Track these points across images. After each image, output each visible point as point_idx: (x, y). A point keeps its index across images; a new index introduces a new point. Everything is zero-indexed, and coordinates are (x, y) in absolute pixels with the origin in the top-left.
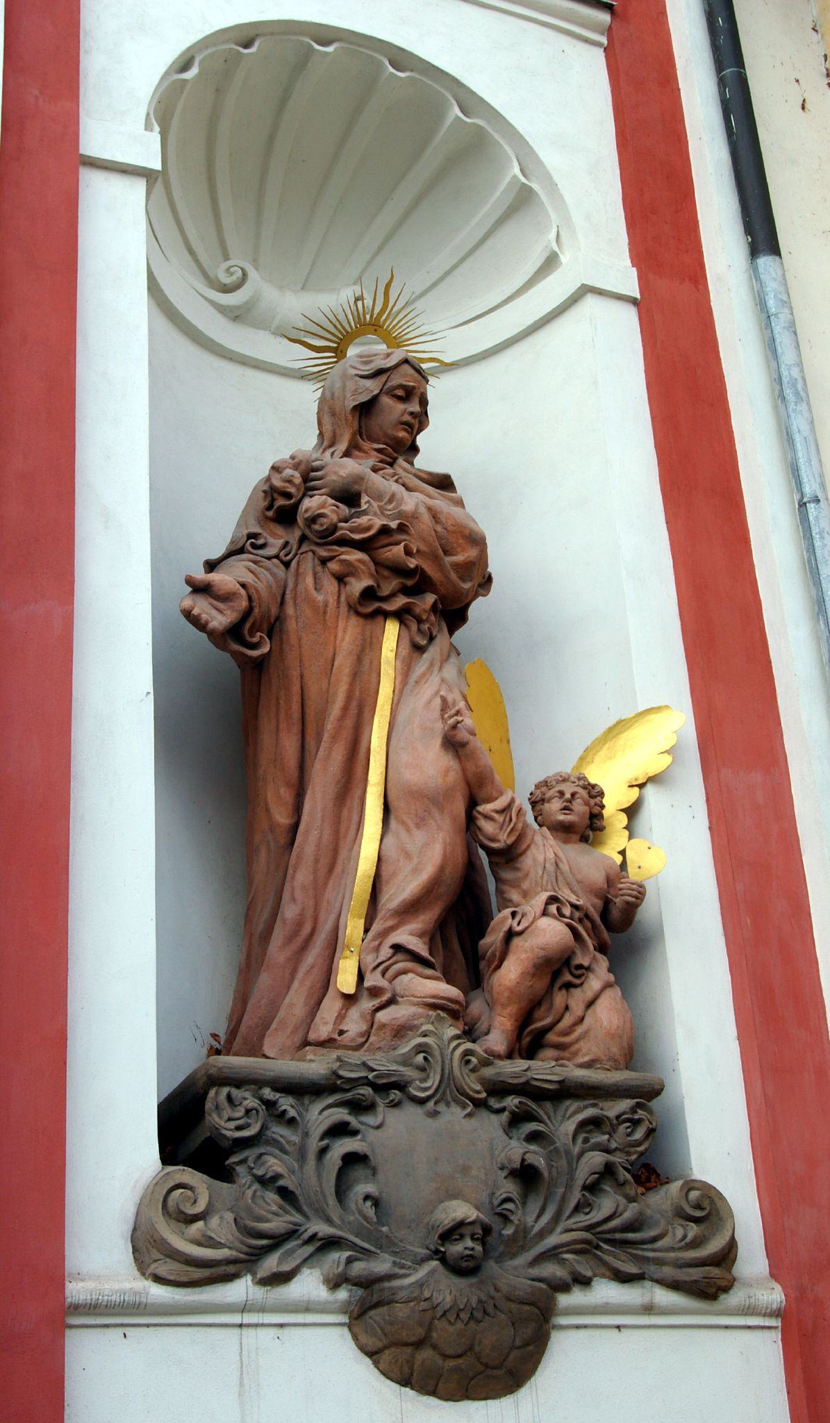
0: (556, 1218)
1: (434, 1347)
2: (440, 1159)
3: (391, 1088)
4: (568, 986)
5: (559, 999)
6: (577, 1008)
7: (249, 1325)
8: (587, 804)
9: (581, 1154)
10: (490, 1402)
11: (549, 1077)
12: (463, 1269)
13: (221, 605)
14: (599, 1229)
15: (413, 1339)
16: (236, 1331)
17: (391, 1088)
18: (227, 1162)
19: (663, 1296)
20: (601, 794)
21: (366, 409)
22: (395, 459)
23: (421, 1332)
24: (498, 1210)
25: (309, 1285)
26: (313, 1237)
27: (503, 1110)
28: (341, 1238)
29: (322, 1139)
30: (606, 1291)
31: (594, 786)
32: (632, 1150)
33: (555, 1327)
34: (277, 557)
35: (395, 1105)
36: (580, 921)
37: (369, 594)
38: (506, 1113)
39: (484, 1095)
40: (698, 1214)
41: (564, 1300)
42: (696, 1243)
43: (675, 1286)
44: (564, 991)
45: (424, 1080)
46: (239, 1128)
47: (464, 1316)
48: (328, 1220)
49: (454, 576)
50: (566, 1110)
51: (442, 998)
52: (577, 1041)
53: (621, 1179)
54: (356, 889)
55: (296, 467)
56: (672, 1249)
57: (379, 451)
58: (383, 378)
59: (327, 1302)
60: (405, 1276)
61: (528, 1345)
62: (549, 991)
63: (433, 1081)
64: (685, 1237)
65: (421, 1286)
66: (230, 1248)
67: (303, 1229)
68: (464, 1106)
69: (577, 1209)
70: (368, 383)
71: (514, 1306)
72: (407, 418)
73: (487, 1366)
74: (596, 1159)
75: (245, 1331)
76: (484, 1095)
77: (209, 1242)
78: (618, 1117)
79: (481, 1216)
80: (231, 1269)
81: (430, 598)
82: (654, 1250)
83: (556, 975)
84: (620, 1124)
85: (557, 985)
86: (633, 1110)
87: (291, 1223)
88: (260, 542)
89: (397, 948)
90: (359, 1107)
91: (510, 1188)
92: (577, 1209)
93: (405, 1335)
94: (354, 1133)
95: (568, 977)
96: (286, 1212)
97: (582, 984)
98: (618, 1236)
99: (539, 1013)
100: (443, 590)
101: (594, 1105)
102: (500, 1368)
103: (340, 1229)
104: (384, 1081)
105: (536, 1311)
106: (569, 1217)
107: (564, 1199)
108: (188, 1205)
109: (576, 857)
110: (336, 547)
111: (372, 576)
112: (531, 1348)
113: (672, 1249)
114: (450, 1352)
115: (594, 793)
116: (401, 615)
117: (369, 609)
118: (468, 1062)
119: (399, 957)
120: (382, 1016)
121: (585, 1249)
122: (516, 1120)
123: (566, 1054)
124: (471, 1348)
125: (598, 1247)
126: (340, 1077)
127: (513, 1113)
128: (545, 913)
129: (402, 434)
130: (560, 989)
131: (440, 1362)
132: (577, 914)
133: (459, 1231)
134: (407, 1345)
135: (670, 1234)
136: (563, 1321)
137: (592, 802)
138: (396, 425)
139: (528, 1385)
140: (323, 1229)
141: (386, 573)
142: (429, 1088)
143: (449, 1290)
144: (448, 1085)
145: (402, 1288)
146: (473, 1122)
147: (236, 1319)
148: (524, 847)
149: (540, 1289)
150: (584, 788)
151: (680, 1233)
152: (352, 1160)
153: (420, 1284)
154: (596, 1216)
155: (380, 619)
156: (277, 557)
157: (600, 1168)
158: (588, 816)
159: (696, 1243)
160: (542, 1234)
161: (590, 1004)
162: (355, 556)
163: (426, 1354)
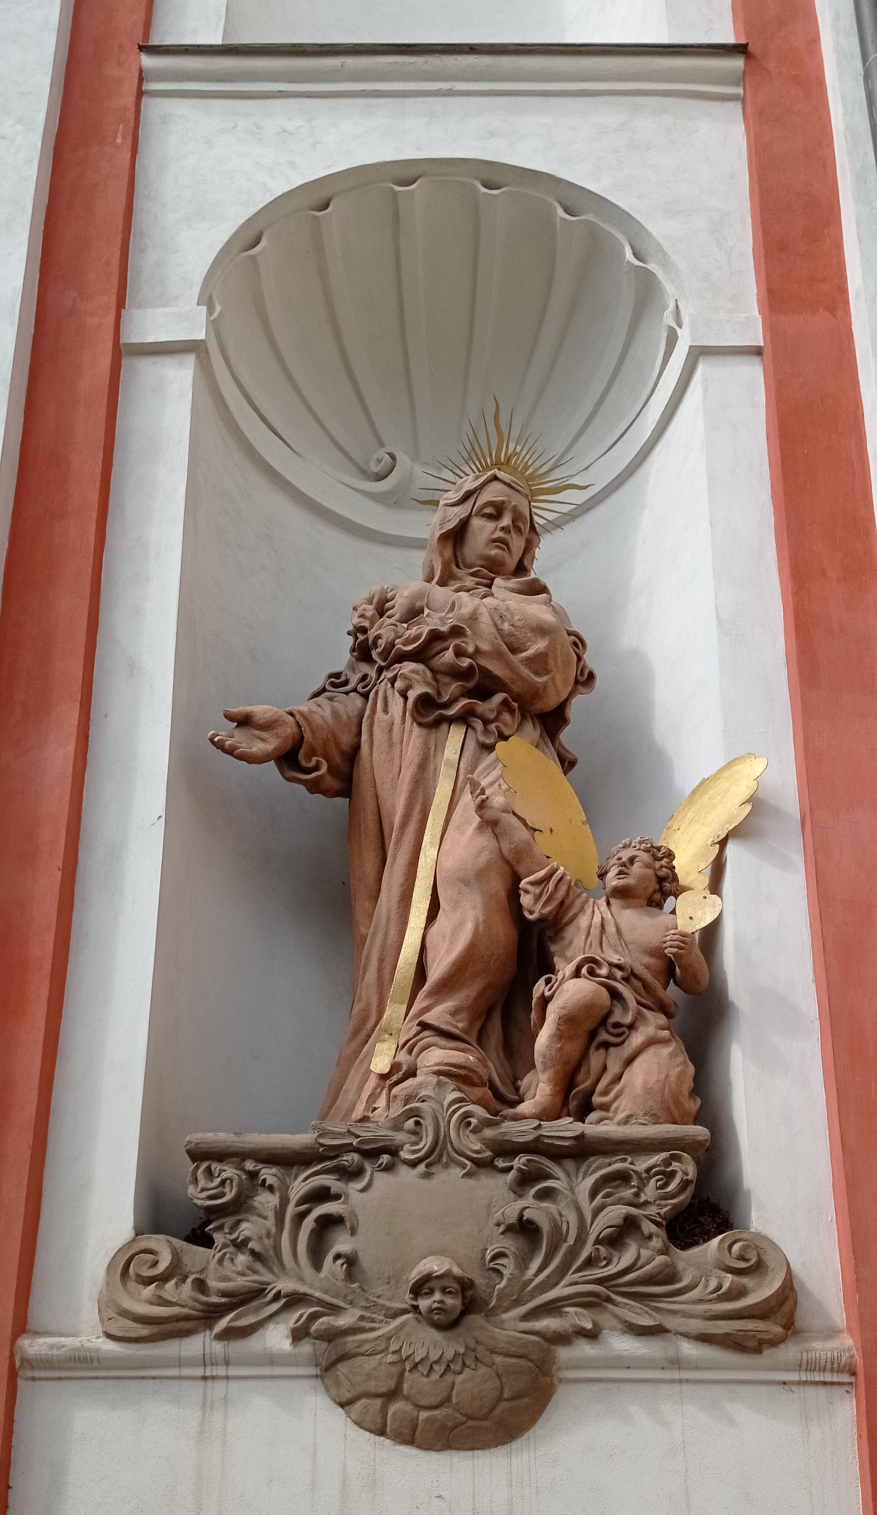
0: (563, 1270)
1: (407, 1398)
2: (424, 1220)
3: (380, 1153)
4: (606, 1045)
5: (596, 1059)
6: (613, 1068)
7: (213, 1378)
8: (647, 866)
9: (602, 1208)
10: (480, 1453)
11: (562, 1134)
12: (448, 1324)
13: (264, 735)
14: (612, 1283)
15: (384, 1390)
16: (201, 1383)
17: (380, 1153)
18: (207, 1229)
19: (689, 1349)
20: (670, 855)
21: (457, 536)
23: (392, 1384)
24: (492, 1265)
25: (277, 1337)
26: (277, 1297)
28: (306, 1294)
29: (298, 1204)
30: (623, 1345)
31: (659, 849)
32: (663, 1202)
33: (561, 1381)
35: (388, 1168)
36: (626, 980)
37: (425, 703)
38: (513, 1171)
39: (489, 1153)
40: (742, 1265)
41: (563, 1353)
42: (738, 1293)
43: (704, 1338)
44: (602, 1051)
45: (417, 1143)
46: (211, 1198)
47: (439, 1369)
48: (301, 1279)
49: (525, 672)
50: (589, 1167)
51: (446, 1064)
52: (616, 1097)
53: (646, 1232)
55: (370, 602)
56: (701, 1301)
58: (471, 502)
59: (289, 1355)
60: (373, 1329)
62: (584, 1056)
63: (427, 1142)
64: (719, 1287)
65: (389, 1339)
66: (190, 1308)
67: (270, 1287)
68: (464, 1166)
69: (590, 1262)
70: (456, 510)
71: (498, 1359)
72: (499, 534)
73: (470, 1417)
74: (615, 1213)
75: (210, 1383)
76: (489, 1153)
77: (163, 1302)
78: (648, 1170)
79: (456, 1270)
80: (186, 1325)
81: (498, 698)
83: (593, 1034)
84: (651, 1178)
85: (594, 1045)
86: (667, 1162)
87: (255, 1282)
90: (351, 1174)
91: (509, 1244)
92: (590, 1262)
93: (372, 1386)
94: (337, 1197)
95: (604, 1036)
96: (255, 1272)
97: (623, 1042)
98: (634, 1289)
99: (580, 1077)
100: (515, 688)
101: (625, 1160)
102: (485, 1418)
103: (311, 1287)
105: (531, 1364)
106: (578, 1270)
107: (574, 1252)
108: (145, 1268)
109: (634, 922)
110: (397, 665)
111: (427, 684)
112: (525, 1400)
113: (701, 1301)
114: (425, 1402)
115: (660, 855)
116: (464, 718)
117: (431, 718)
118: (469, 1124)
119: (426, 1033)
120: (395, 1091)
121: (591, 1302)
122: (525, 1180)
123: (610, 1114)
124: (448, 1399)
125: (609, 1300)
126: (322, 1145)
127: (520, 1170)
128: (577, 974)
129: (494, 552)
130: (598, 1048)
131: (415, 1413)
132: (619, 974)
134: (377, 1396)
136: (571, 1374)
137: (658, 865)
138: (487, 544)
140: (286, 1285)
141: (446, 680)
143: (427, 1342)
144: (444, 1147)
145: (365, 1341)
146: (471, 1182)
147: (199, 1372)
148: (571, 914)
149: (533, 1342)
150: (647, 851)
151: (713, 1284)
152: (328, 1223)
153: (388, 1338)
154: (612, 1270)
155: (444, 727)
157: (620, 1221)
158: (654, 878)
159: (738, 1293)
160: (543, 1287)
162: (408, 667)
163: (397, 1407)
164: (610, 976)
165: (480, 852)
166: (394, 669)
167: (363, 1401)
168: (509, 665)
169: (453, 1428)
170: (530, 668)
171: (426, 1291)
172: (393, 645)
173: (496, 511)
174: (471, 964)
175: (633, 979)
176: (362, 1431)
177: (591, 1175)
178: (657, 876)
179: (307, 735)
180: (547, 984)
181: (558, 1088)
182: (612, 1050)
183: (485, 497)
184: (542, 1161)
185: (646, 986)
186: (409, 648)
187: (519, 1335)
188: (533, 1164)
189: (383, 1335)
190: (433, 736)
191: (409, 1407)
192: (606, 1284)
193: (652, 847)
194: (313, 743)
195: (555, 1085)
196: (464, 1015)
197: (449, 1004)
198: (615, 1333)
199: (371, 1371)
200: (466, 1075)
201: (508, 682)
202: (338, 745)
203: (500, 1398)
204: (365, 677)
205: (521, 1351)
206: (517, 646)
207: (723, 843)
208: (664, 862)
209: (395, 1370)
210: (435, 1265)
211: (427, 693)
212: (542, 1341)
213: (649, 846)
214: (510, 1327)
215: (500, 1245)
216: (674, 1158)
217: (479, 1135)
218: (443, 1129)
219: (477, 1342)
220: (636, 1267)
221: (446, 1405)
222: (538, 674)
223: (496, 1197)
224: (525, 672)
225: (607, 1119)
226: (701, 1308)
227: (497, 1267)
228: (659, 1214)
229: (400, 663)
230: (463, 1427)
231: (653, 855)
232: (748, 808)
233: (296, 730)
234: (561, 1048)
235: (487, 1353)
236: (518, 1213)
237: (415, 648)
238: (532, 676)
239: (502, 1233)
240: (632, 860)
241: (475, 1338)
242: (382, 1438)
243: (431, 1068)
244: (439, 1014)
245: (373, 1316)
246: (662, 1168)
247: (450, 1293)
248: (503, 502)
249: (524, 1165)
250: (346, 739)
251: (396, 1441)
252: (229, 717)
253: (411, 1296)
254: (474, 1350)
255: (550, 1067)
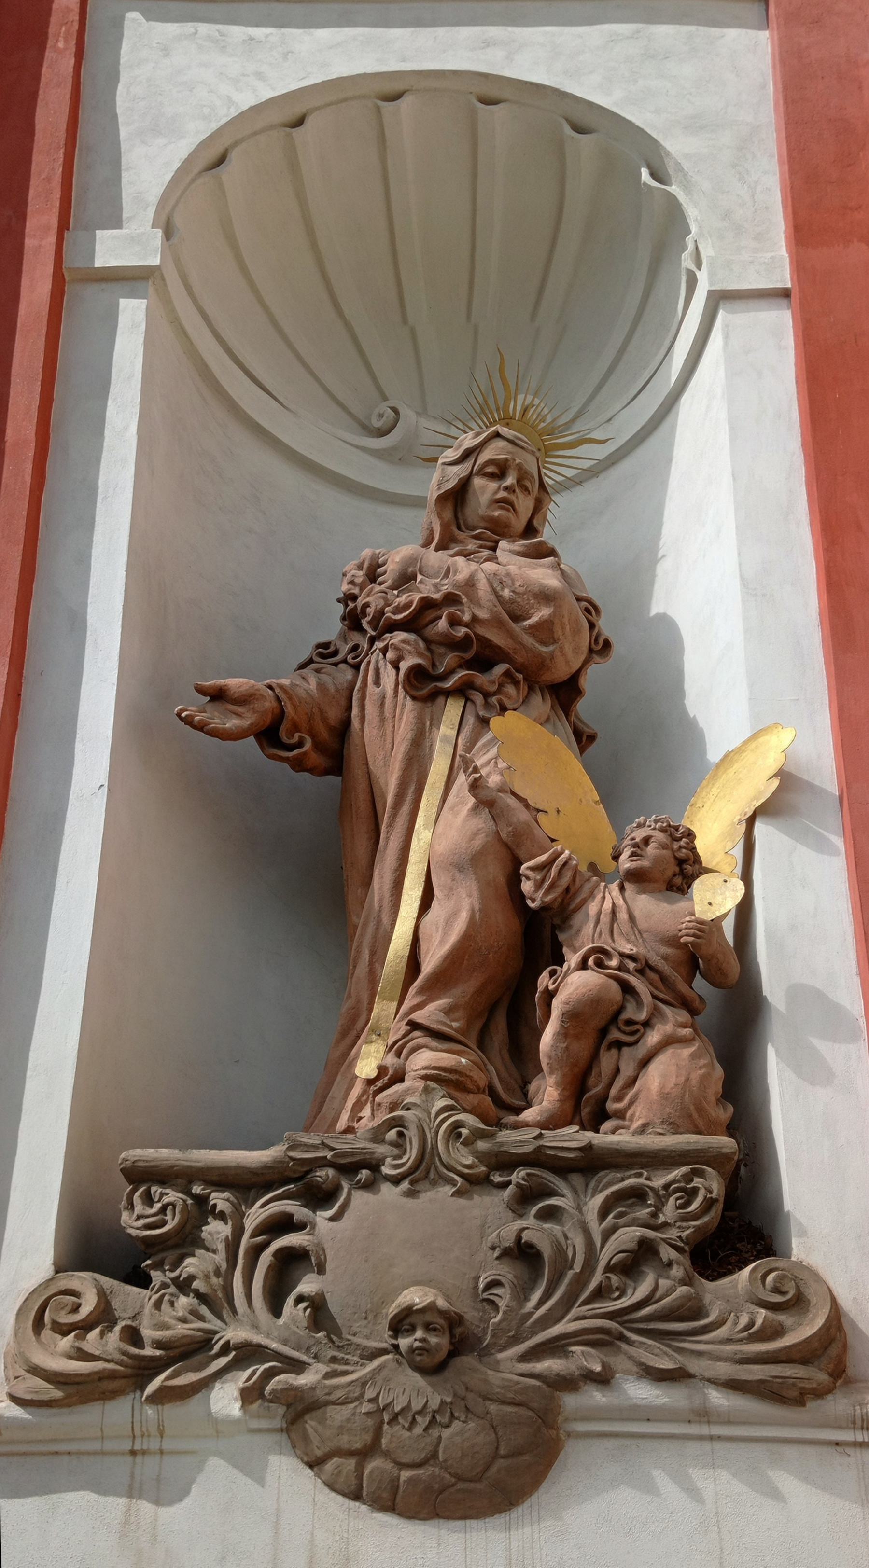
0: (568, 1303)
1: (387, 1454)
4: (619, 1045)
5: (607, 1060)
6: (627, 1069)
8: (664, 847)
9: (613, 1229)
11: (566, 1144)
12: (433, 1368)
13: (240, 709)
14: (626, 1318)
15: (358, 1446)
17: (361, 1169)
20: (690, 835)
21: (457, 497)
22: (497, 542)
23: (368, 1438)
24: (485, 1295)
27: (505, 1185)
31: (677, 828)
32: (684, 1224)
33: (569, 1435)
34: (345, 661)
35: (369, 1186)
36: (640, 972)
41: (570, 1401)
42: (773, 1332)
43: (734, 1385)
44: (614, 1051)
45: (400, 1157)
49: (528, 640)
51: (435, 1068)
52: (631, 1103)
54: (386, 970)
55: (360, 567)
56: (729, 1341)
57: (476, 537)
60: (346, 1373)
61: (520, 1454)
62: (594, 1057)
63: (411, 1155)
64: (751, 1324)
65: (364, 1384)
68: (453, 1183)
69: (600, 1294)
70: (455, 469)
71: (493, 1408)
73: (460, 1478)
74: (628, 1236)
76: (483, 1169)
78: (666, 1187)
79: (441, 1303)
81: (500, 669)
82: (707, 1343)
83: (603, 1032)
84: (670, 1196)
86: (688, 1178)
88: (332, 648)
89: (414, 1026)
91: (506, 1272)
92: (600, 1294)
93: (344, 1441)
95: (615, 1034)
97: (637, 1042)
99: (591, 1080)
100: (519, 659)
101: (640, 1175)
102: (478, 1479)
104: (348, 1160)
105: (531, 1413)
106: (586, 1302)
107: (581, 1280)
109: (648, 907)
110: (387, 635)
111: (420, 655)
112: (526, 1457)
113: (729, 1341)
114: (406, 1459)
115: (678, 834)
116: (463, 691)
117: (425, 692)
118: (459, 1135)
119: (417, 1033)
120: (378, 1098)
121: (601, 1340)
122: (526, 1197)
123: (626, 1123)
124: (434, 1455)
125: (622, 1338)
127: (518, 1185)
128: (583, 965)
130: (609, 1047)
131: (395, 1472)
132: (631, 965)
133: (408, 1321)
134: (351, 1453)
135: (729, 1323)
137: (676, 846)
139: (526, 1504)
141: (442, 650)
142: (403, 1165)
143: (410, 1389)
145: (336, 1387)
146: (462, 1202)
148: (578, 900)
149: (534, 1386)
150: (663, 830)
151: (744, 1320)
153: (363, 1383)
154: (625, 1302)
155: (441, 700)
156: (345, 661)
157: (633, 1245)
158: (672, 860)
159: (773, 1332)
161: (645, 1063)
162: (399, 637)
163: (374, 1464)
164: (621, 968)
165: (476, 834)
166: (384, 639)
167: (336, 1460)
168: (511, 634)
169: (441, 1492)
170: (534, 636)
171: (406, 1327)
172: (381, 613)
173: (499, 470)
174: (467, 957)
175: (648, 971)
176: (333, 1495)
177: (601, 1191)
178: (675, 858)
179: (289, 709)
180: (551, 977)
181: (567, 1093)
182: (625, 1050)
183: (486, 455)
184: (544, 1175)
185: (663, 978)
186: (399, 617)
187: (516, 1378)
188: (534, 1178)
189: (357, 1380)
190: (428, 710)
191: (388, 1465)
192: (619, 1319)
193: (669, 826)
194: (296, 718)
195: (563, 1089)
196: (459, 1014)
197: (442, 1002)
198: (630, 1377)
199: (342, 1423)
200: (457, 1080)
201: (511, 652)
202: (324, 720)
203: (495, 1456)
204: (355, 648)
205: (519, 1398)
206: (519, 613)
207: (751, 822)
208: (683, 842)
209: (370, 1422)
210: (416, 1296)
211: (419, 665)
212: (544, 1386)
213: (665, 825)
214: (508, 1367)
215: (494, 1272)
216: (696, 1173)
217: (470, 1147)
218: (429, 1141)
219: (467, 1388)
220: (653, 1300)
221: (431, 1462)
222: (543, 643)
223: (492, 1217)
224: (528, 640)
225: (623, 1128)
226: (729, 1348)
227: (492, 1297)
228: (680, 1237)
229: (391, 632)
230: (452, 1490)
231: (671, 835)
232: (776, 783)
233: (275, 704)
234: (567, 1048)
235: (480, 1399)
236: (515, 1234)
237: (405, 617)
238: (537, 645)
239: (498, 1258)
240: (646, 841)
241: (465, 1384)
242: (357, 1504)
243: (418, 1072)
244: (430, 1013)
245: (346, 1357)
246: (682, 1184)
247: (435, 1330)
248: (506, 460)
249: (523, 1179)
250: (334, 714)
251: (374, 1508)
252: (201, 690)
253: (390, 1333)
254: (463, 1399)
255: (557, 1069)
